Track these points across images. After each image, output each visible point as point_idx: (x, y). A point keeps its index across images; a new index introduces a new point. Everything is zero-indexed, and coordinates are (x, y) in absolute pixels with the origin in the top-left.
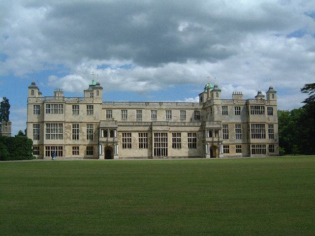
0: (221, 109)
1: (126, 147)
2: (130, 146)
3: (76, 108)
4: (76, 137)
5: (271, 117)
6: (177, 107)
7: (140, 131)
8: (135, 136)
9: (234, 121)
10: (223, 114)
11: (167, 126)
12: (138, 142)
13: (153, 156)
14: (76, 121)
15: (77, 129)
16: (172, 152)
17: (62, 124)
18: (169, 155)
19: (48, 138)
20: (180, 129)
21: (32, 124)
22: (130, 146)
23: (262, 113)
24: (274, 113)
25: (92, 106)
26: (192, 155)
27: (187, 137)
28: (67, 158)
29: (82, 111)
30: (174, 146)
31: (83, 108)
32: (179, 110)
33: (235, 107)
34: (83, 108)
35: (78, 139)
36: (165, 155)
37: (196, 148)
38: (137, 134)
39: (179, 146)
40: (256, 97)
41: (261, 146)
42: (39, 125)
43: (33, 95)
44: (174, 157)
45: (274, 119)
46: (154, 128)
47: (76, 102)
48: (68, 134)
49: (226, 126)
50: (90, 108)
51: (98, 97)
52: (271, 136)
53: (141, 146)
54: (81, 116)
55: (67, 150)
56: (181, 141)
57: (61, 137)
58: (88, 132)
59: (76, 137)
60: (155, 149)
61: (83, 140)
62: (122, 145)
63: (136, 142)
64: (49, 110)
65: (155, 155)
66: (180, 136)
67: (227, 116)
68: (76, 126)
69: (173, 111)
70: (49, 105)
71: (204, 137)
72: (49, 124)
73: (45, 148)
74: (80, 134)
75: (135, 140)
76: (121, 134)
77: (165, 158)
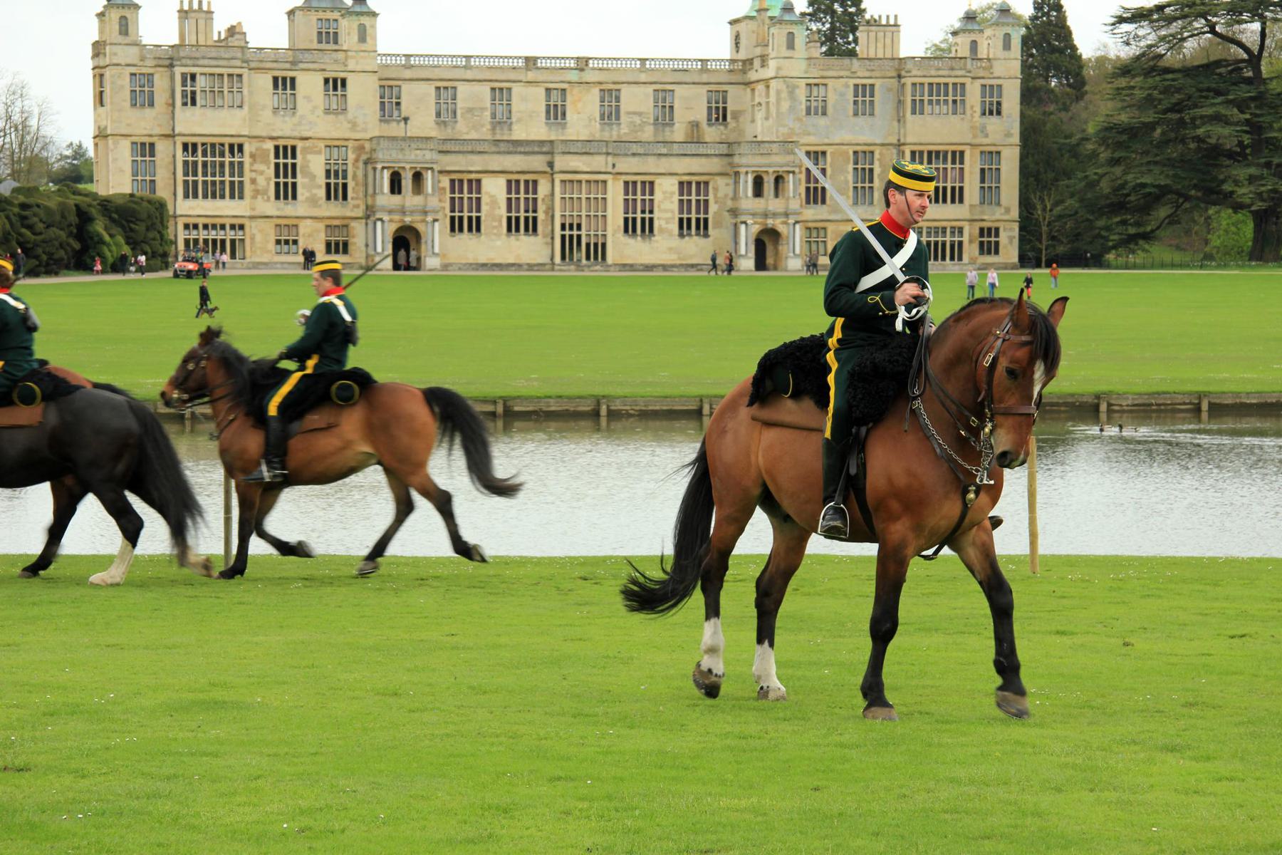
0: (802, 94)
1: (461, 230)
2: (475, 226)
3: (284, 84)
4: (286, 191)
5: (993, 123)
6: (643, 78)
7: (512, 172)
8: (495, 189)
9: (848, 137)
10: (808, 112)
11: (608, 154)
12: (503, 212)
13: (558, 259)
14: (288, 133)
15: (290, 161)
16: (622, 248)
17: (241, 147)
18: (610, 260)
19: (191, 191)
20: (651, 165)
21: (125, 145)
22: (475, 226)
23: (957, 106)
24: (1005, 106)
25: (344, 82)
26: (694, 261)
27: (676, 198)
28: (256, 265)
29: (308, 98)
30: (629, 227)
31: (310, 85)
32: (650, 89)
33: (856, 86)
34: (310, 85)
35: (294, 197)
36: (596, 258)
37: (706, 235)
38: (501, 182)
39: (648, 228)
40: (955, 33)
41: (944, 230)
42: (152, 145)
43: (126, 34)
44: (631, 267)
45: (1005, 132)
46: (561, 162)
47: (288, 66)
48: (261, 181)
49: (816, 156)
50: (336, 84)
51: (364, 47)
52: (990, 193)
53: (513, 226)
54: (302, 117)
55: (258, 238)
56: (656, 210)
57: (237, 191)
58: (328, 172)
59: (286, 191)
60: (563, 237)
61: (313, 201)
62: (448, 221)
63: (497, 212)
64: (193, 93)
65: (563, 257)
66: (652, 193)
67: (822, 121)
68: (286, 151)
69: (626, 92)
70: (193, 77)
71: (735, 197)
72: (195, 145)
73: (180, 227)
74: (300, 180)
75: (494, 202)
76: (445, 182)
77: (597, 271)
